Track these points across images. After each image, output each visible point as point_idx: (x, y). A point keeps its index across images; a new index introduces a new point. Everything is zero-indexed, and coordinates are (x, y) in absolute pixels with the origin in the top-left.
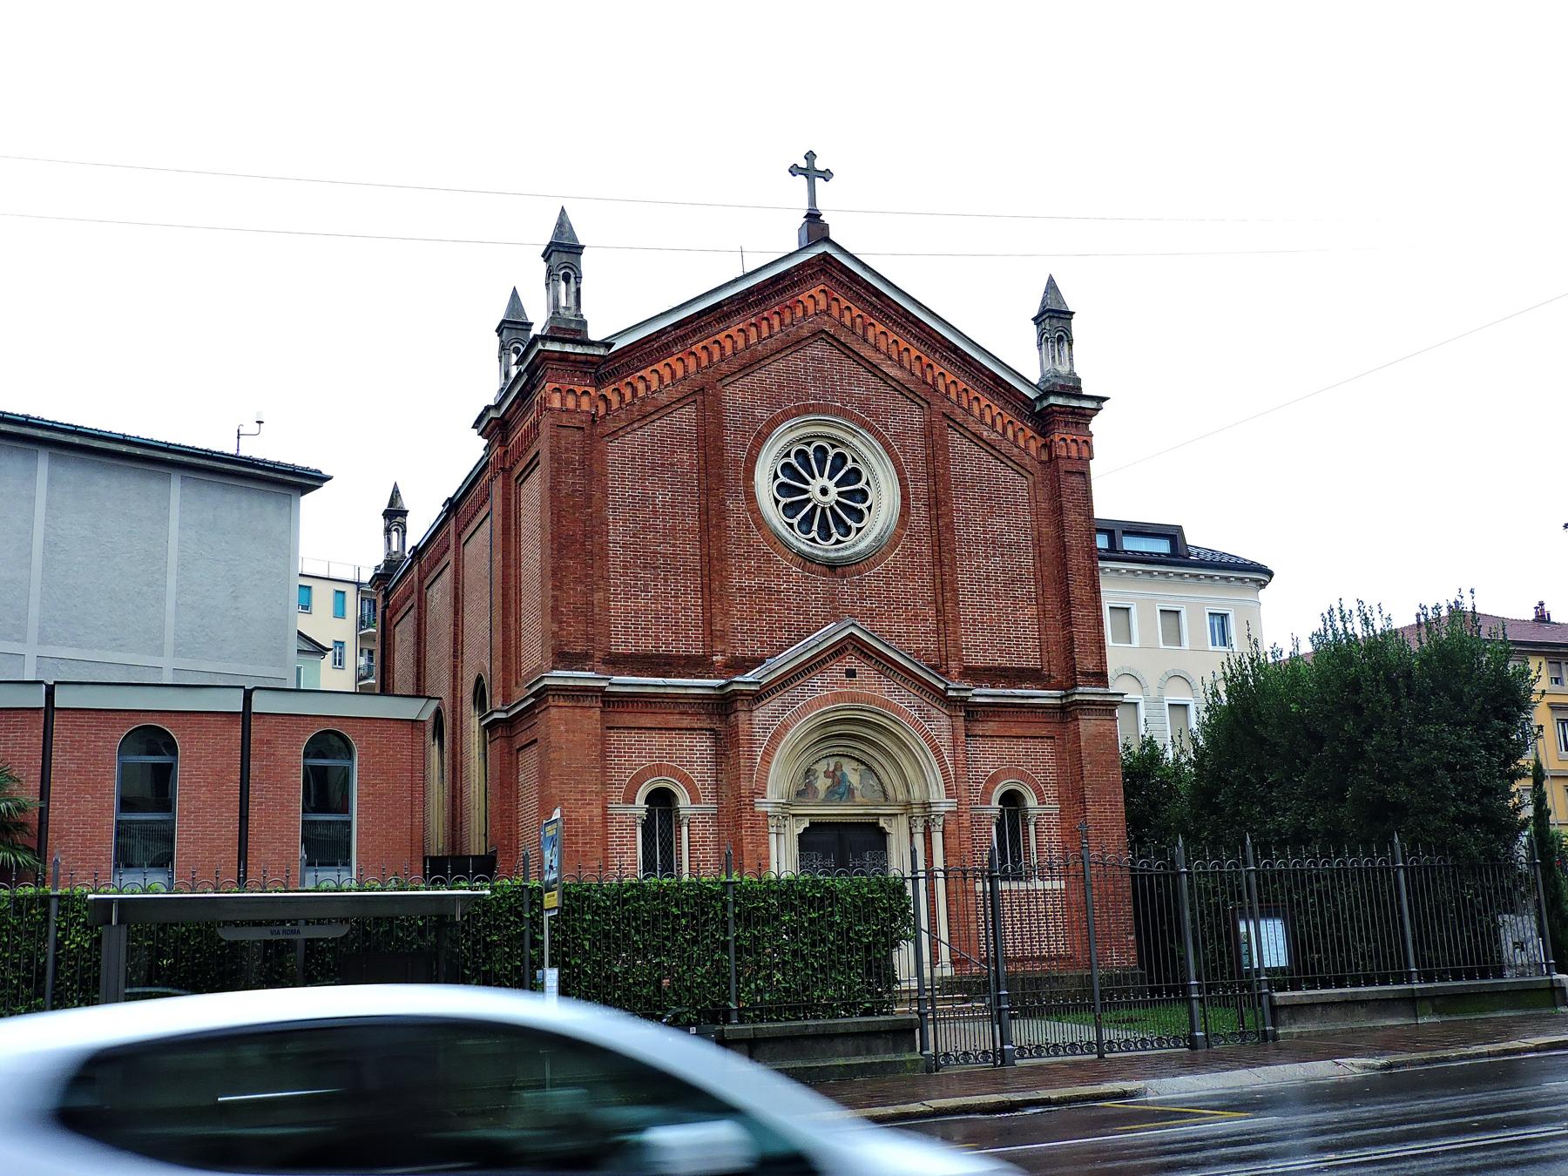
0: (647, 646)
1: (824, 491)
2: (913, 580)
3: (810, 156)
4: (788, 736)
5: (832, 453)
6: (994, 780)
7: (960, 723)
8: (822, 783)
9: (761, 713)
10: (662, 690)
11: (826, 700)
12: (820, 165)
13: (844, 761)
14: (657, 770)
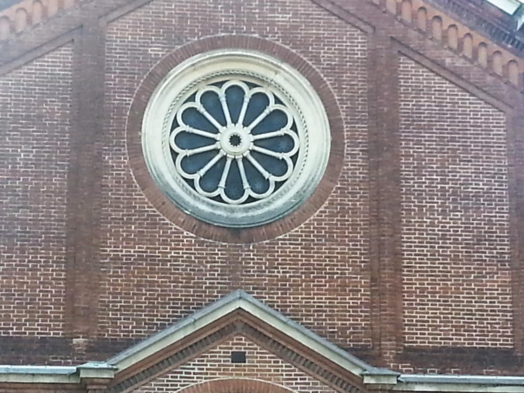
1: (235, 140)
5: (249, 93)
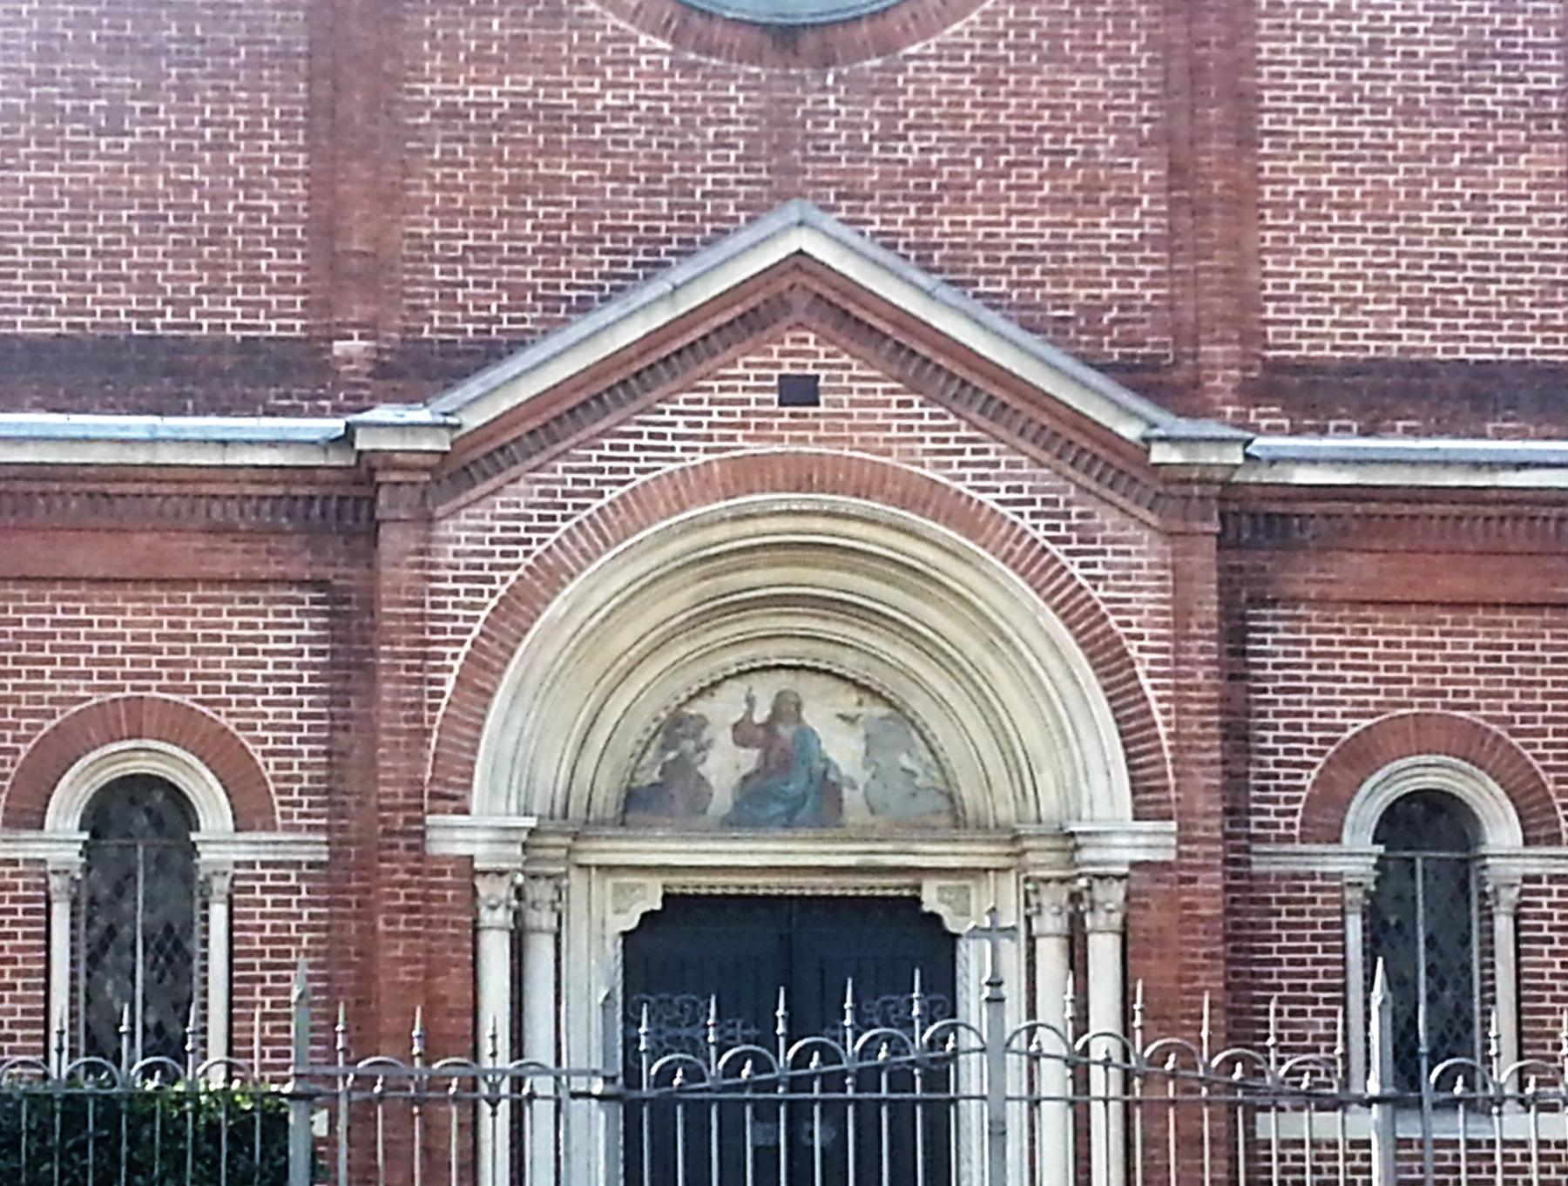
0: (114, 309)
2: (1088, 66)
4: (557, 607)
6: (1359, 757)
7: (1204, 559)
8: (725, 766)
9: (462, 531)
10: (141, 456)
11: (700, 484)
13: (808, 687)
14: (131, 719)
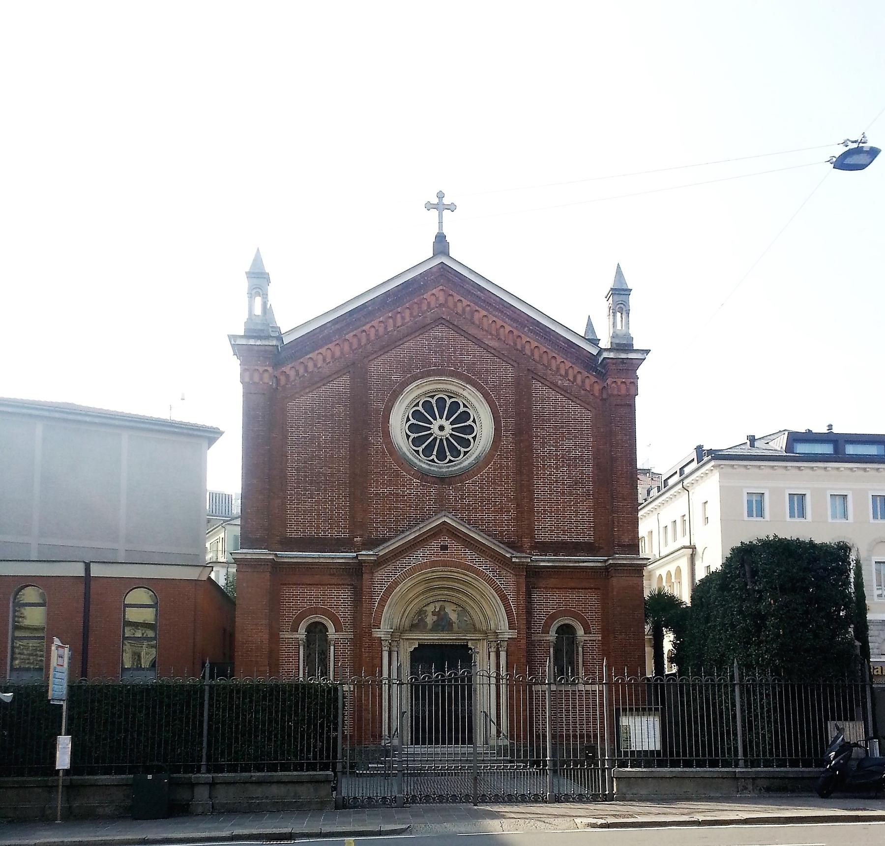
0: (312, 532)
1: (442, 428)
3: (440, 195)
5: (449, 402)
6: (553, 618)
7: (523, 580)
8: (430, 619)
9: (379, 575)
12: (446, 201)
14: (315, 611)
